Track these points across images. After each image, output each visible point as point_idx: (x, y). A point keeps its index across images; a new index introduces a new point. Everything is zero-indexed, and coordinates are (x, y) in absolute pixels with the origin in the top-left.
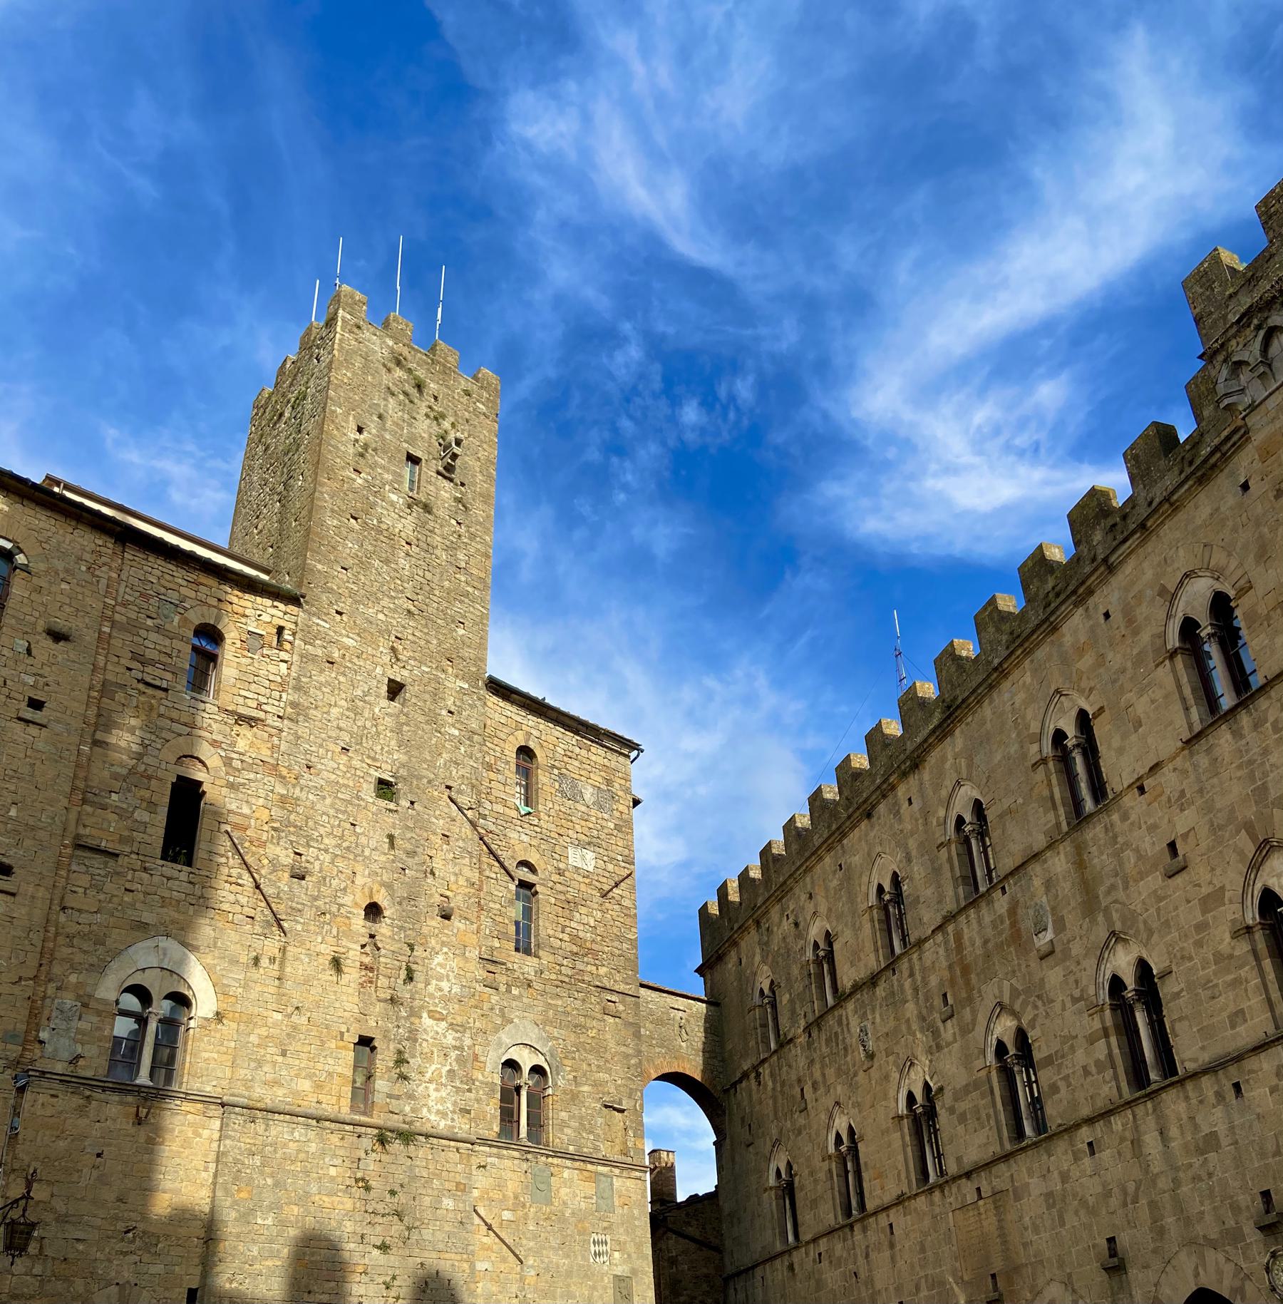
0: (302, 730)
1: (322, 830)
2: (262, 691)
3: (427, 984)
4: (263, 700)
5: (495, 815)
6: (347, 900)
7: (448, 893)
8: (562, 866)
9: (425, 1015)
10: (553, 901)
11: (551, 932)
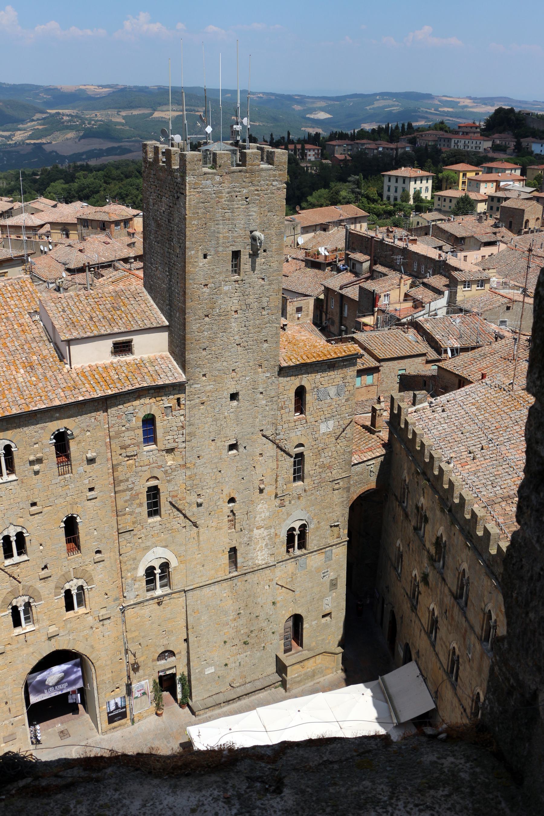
0: (194, 442)
2: (175, 433)
3: (255, 517)
4: (176, 437)
5: (284, 430)
6: (220, 503)
7: (263, 478)
8: (316, 436)
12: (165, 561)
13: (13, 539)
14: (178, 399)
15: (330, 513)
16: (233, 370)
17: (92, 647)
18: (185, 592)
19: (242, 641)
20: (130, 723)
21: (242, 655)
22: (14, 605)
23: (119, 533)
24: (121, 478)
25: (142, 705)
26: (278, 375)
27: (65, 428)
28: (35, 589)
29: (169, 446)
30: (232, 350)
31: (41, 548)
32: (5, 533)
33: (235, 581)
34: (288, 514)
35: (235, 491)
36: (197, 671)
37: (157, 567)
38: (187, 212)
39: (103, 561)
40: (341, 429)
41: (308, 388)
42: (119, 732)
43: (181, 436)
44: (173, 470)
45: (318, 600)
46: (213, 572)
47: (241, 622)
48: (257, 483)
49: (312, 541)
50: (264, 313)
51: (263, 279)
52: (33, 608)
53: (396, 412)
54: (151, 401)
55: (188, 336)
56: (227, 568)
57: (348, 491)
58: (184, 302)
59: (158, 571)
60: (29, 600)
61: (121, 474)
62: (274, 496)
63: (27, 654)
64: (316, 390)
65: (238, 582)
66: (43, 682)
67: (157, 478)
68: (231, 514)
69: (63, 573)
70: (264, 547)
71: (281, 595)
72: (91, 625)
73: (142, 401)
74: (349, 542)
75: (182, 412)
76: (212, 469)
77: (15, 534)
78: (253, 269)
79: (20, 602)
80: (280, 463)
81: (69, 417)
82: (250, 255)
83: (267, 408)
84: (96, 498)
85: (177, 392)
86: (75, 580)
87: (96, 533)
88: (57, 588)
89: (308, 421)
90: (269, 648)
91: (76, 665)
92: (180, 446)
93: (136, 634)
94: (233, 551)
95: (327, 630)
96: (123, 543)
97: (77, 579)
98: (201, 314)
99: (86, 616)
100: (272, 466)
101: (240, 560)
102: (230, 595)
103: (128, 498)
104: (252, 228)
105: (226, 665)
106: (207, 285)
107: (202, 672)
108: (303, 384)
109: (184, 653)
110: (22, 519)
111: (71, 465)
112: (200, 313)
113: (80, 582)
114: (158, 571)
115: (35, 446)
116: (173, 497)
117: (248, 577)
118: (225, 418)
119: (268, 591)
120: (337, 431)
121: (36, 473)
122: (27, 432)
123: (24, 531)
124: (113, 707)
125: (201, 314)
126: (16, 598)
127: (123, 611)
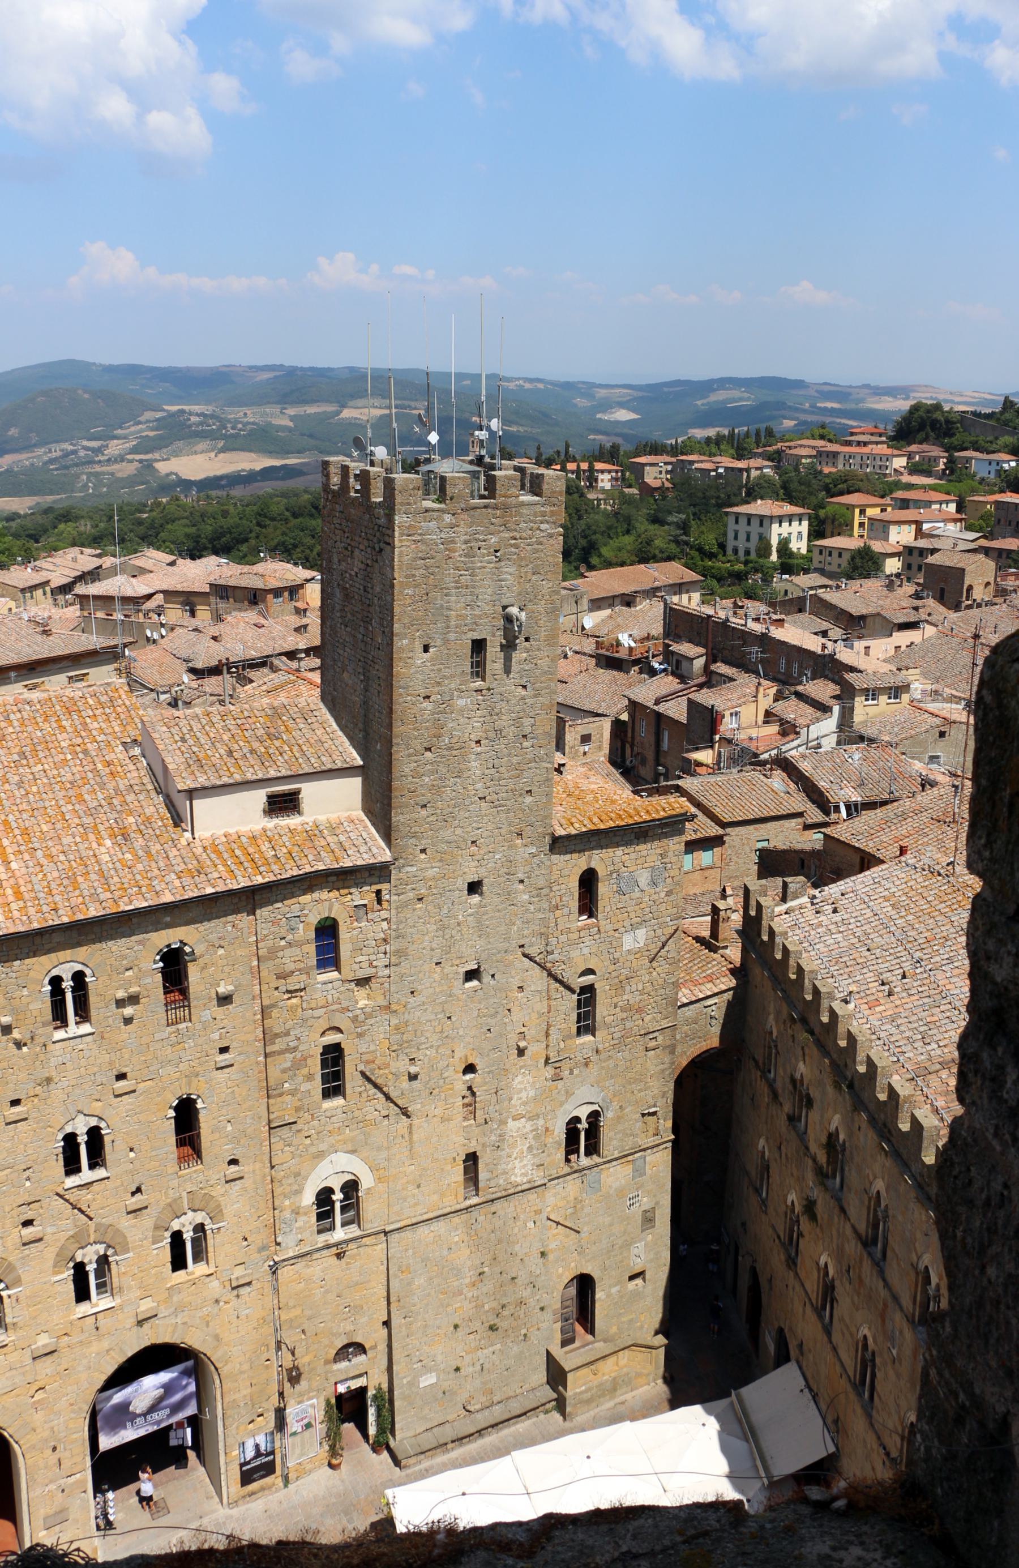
0: (405, 967)
1: (428, 1035)
3: (511, 1099)
5: (561, 945)
6: (449, 1073)
7: (524, 1029)
8: (617, 955)
9: (510, 1120)
10: (608, 987)
11: (605, 1013)
12: (351, 1177)
13: (82, 1139)
14: (378, 893)
15: (640, 1091)
16: (473, 842)
17: (217, 1338)
18: (386, 1233)
19: (487, 1325)
20: (281, 1485)
21: (485, 1351)
22: (79, 1260)
23: (270, 1128)
24: (277, 1030)
25: (303, 1448)
26: (551, 850)
27: (181, 942)
28: (118, 1230)
29: (361, 974)
30: (471, 808)
31: (132, 1155)
32: (69, 1129)
33: (475, 1213)
34: (567, 1092)
35: (475, 1053)
36: (405, 1381)
37: (337, 1189)
38: (396, 575)
39: (242, 1178)
40: (660, 944)
41: (601, 872)
42: (259, 1501)
43: (382, 956)
44: (368, 1016)
45: (620, 1248)
46: (436, 1197)
47: (485, 1290)
48: (513, 1039)
49: (610, 1141)
50: (526, 744)
51: (524, 687)
52: (113, 1266)
53: (753, 913)
54: (331, 894)
55: (395, 784)
56: (461, 1190)
57: (672, 1052)
58: (390, 726)
59: (338, 1196)
60: (106, 1251)
61: (277, 1022)
62: (543, 1061)
63: (97, 1354)
64: (615, 875)
65: (481, 1216)
66: (124, 1408)
67: (339, 1030)
68: (468, 1093)
69: (169, 1200)
70: (523, 1154)
71: (556, 1239)
72: (217, 1296)
73: (316, 895)
74: (674, 1142)
75: (384, 914)
76: (436, 1014)
77: (85, 1130)
78: (507, 670)
79: (89, 1256)
80: (553, 1003)
81: (187, 923)
82: (502, 646)
83: (532, 907)
84: (232, 1065)
85: (376, 880)
86: (190, 1214)
87: (229, 1128)
88: (156, 1228)
89: (602, 930)
90: (535, 1337)
91: (186, 1373)
92: (380, 974)
93: (297, 1312)
94: (472, 1160)
95: (636, 1307)
96: (277, 1146)
97: (194, 1211)
98: (419, 747)
99: (208, 1279)
100: (537, 1008)
101: (483, 1175)
102: (466, 1239)
103: (288, 1064)
104: (505, 602)
105: (457, 1369)
106: (428, 697)
107: (413, 1384)
108: (593, 865)
109: (383, 1347)
110: (100, 1104)
111: (189, 1006)
112: (418, 745)
113: (200, 1218)
114: (338, 1196)
115: (127, 973)
116: (368, 1062)
117: (497, 1206)
118: (459, 924)
119: (533, 1231)
120: (652, 947)
121: (128, 1021)
122: (114, 949)
123: (103, 1125)
124: (250, 1453)
125: (419, 747)
126: (82, 1248)
127: (274, 1270)
